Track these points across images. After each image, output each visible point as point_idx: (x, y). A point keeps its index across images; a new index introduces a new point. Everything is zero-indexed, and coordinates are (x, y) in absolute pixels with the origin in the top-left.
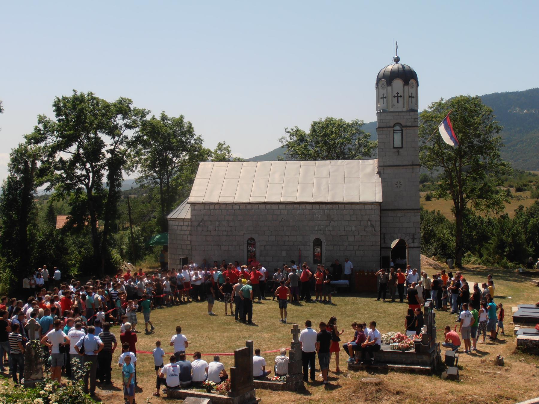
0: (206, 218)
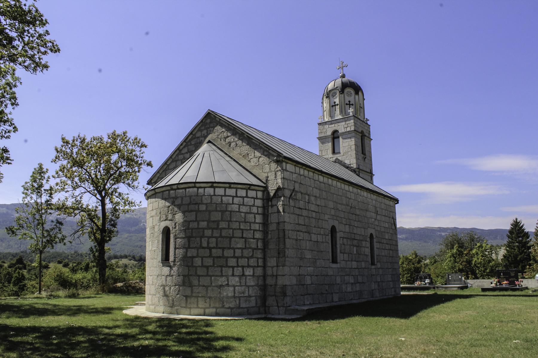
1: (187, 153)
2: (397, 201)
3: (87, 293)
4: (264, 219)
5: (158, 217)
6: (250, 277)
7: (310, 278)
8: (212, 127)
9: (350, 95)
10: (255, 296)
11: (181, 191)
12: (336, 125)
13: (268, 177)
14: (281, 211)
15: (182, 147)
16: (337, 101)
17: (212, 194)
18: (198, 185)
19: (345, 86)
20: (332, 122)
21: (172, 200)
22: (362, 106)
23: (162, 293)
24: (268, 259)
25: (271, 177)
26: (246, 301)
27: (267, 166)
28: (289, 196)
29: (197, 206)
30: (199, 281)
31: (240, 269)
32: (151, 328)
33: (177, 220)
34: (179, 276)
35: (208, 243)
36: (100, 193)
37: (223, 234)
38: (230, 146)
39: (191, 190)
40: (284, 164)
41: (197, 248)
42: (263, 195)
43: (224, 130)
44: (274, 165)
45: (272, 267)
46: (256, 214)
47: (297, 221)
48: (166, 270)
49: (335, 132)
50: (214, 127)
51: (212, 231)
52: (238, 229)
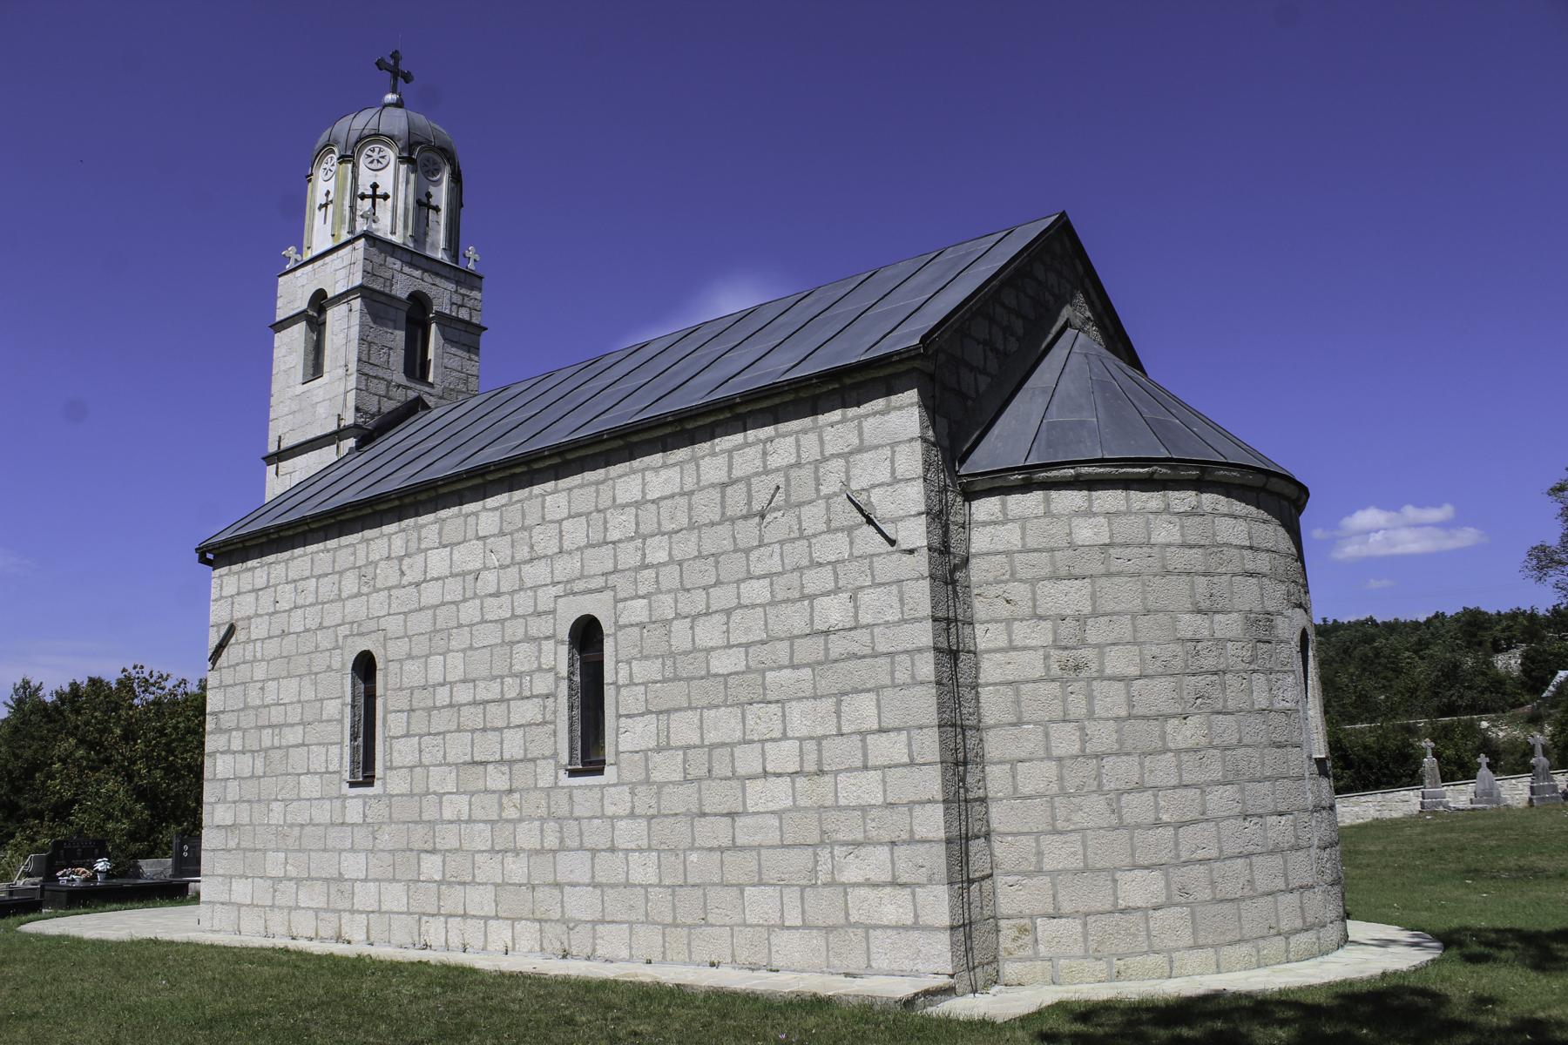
20: (416, 260)
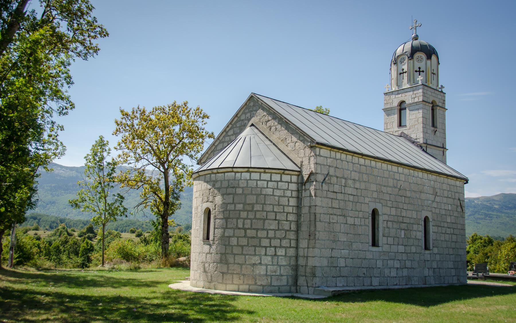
0: (332, 171)
1: (232, 135)
2: (466, 181)
3: (149, 267)
4: (298, 202)
5: (201, 199)
6: (282, 257)
7: (344, 260)
8: (255, 111)
9: (420, 60)
10: (286, 275)
11: (220, 175)
12: (403, 95)
13: (302, 162)
14: (313, 195)
15: (228, 129)
16: (405, 67)
17: (248, 178)
18: (235, 170)
19: (414, 50)
20: (399, 92)
21: (213, 183)
22: (435, 72)
23: (202, 269)
24: (301, 240)
25: (306, 162)
26: (277, 280)
27: (302, 151)
28: (322, 181)
29: (234, 190)
30: (234, 259)
31: (273, 249)
32: (182, 300)
33: (217, 202)
34: (217, 254)
35: (244, 224)
36: (163, 164)
37: (258, 216)
38: (270, 130)
39: (229, 173)
40: (318, 149)
41: (234, 229)
42: (298, 179)
43: (265, 113)
44: (308, 150)
45: (304, 249)
46: (290, 197)
47: (330, 204)
48: (206, 248)
49: (402, 102)
50: (256, 111)
51: (248, 213)
52: (271, 212)
